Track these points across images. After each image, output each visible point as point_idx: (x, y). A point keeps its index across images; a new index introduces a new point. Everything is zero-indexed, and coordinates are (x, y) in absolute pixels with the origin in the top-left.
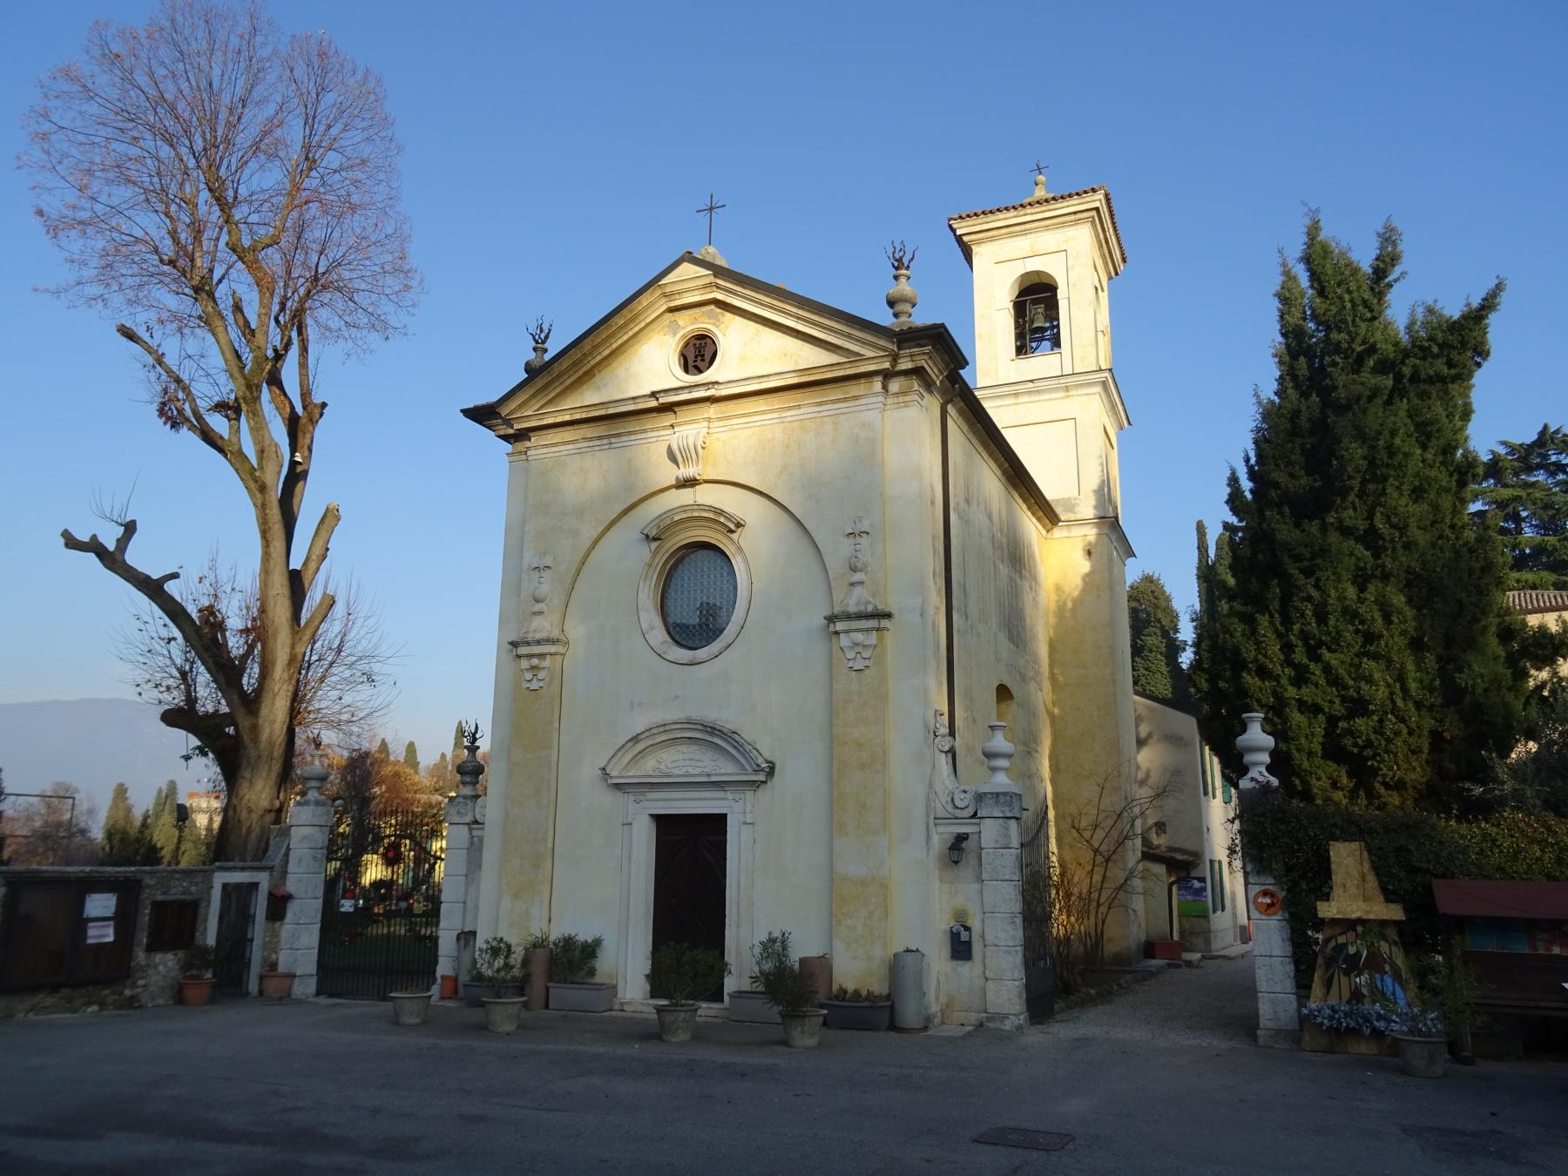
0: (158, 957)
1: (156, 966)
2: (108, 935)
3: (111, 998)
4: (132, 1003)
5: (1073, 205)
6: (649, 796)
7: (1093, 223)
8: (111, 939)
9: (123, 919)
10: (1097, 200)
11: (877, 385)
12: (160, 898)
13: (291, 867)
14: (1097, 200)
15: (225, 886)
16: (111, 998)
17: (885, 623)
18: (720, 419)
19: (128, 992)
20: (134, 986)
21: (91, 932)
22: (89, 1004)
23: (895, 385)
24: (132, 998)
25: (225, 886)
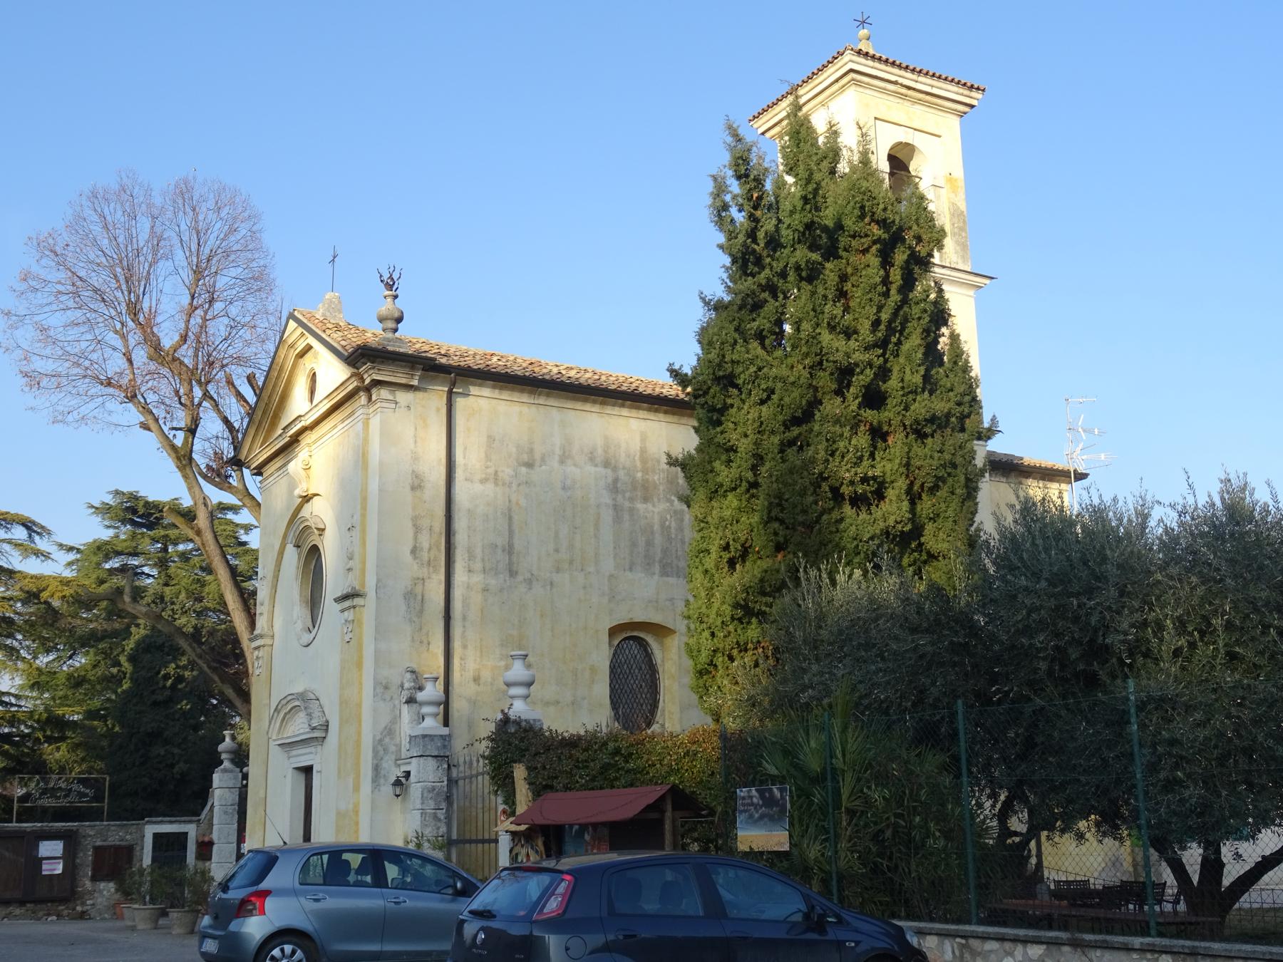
0: (102, 885)
1: (101, 892)
2: (59, 869)
3: (65, 912)
4: (82, 916)
5: (832, 73)
6: (294, 753)
7: (858, 83)
8: (59, 871)
9: (69, 856)
10: (849, 61)
11: (363, 399)
12: (99, 843)
13: (215, 821)
14: (849, 61)
15: (157, 837)
16: (65, 912)
17: (357, 601)
18: (315, 442)
19: (79, 908)
20: (83, 904)
21: (44, 867)
22: (49, 915)
23: (375, 394)
24: (83, 912)
25: (157, 837)
